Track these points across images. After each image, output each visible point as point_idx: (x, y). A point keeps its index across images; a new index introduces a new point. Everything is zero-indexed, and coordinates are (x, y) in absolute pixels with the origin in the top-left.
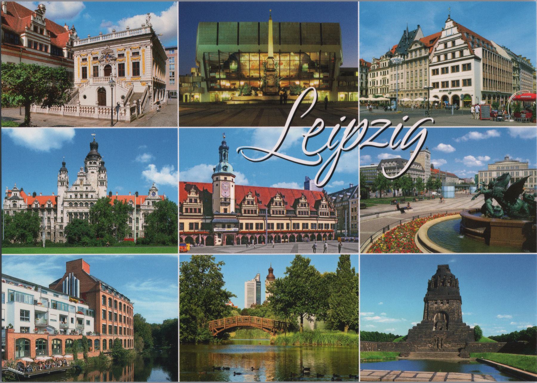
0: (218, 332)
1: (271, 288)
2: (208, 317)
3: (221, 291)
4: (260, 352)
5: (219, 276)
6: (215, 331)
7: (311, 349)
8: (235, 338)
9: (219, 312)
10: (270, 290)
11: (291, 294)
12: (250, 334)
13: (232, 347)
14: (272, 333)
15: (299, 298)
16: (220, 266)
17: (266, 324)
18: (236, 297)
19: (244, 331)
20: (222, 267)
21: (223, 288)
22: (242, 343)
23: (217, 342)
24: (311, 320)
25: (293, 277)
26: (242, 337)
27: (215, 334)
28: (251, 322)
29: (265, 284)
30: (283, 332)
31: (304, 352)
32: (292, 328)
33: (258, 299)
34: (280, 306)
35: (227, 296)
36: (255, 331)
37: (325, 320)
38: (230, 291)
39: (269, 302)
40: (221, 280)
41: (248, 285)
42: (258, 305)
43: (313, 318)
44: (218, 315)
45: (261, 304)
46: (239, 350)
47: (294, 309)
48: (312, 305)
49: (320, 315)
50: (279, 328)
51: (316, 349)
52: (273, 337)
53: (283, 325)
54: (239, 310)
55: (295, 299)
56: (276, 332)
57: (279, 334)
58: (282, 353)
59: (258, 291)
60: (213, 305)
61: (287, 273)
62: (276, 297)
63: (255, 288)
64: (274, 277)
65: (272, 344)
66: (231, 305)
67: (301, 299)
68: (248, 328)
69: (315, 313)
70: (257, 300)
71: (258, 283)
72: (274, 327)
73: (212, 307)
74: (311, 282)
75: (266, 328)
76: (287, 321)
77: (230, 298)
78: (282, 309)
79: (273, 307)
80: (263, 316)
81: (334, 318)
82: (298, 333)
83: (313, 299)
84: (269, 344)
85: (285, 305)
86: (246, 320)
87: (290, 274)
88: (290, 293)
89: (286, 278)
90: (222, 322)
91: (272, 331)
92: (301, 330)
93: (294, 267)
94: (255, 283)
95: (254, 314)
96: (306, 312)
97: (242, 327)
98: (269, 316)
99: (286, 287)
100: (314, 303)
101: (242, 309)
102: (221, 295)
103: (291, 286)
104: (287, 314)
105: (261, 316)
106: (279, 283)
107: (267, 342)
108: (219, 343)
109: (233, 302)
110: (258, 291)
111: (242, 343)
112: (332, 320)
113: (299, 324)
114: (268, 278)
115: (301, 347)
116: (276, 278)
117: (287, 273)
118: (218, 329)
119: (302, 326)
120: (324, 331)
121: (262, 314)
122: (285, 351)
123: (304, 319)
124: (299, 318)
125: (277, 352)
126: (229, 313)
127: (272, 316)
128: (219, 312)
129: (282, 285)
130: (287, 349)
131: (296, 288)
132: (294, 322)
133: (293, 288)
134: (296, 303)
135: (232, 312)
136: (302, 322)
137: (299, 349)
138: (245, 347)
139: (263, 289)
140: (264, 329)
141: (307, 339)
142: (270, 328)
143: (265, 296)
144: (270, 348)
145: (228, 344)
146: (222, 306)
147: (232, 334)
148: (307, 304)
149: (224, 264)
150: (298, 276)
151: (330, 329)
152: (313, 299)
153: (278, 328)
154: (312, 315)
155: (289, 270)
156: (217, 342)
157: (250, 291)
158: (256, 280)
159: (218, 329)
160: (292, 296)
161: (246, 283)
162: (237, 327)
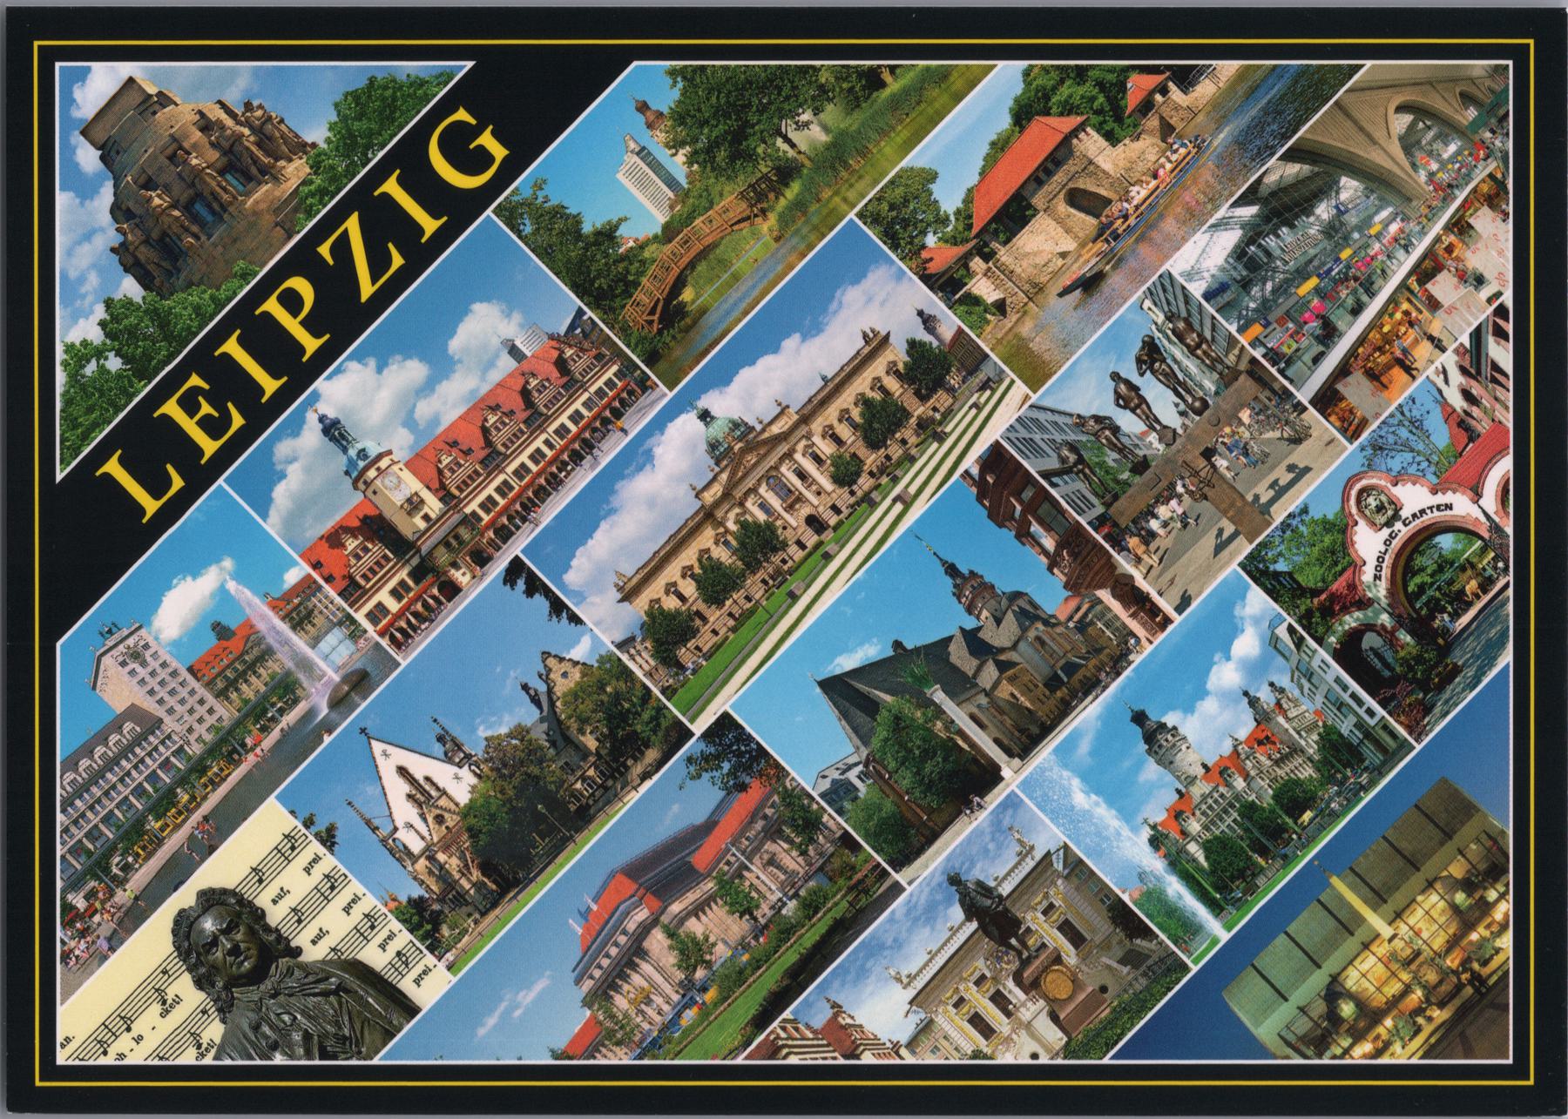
0: (656, 317)
1: (674, 140)
2: (612, 310)
5: (558, 212)
6: (650, 323)
7: (860, 177)
8: (698, 295)
10: (675, 145)
11: (720, 113)
13: (711, 318)
14: (759, 220)
15: (744, 106)
16: (541, 194)
17: (731, 214)
18: (626, 219)
19: (702, 267)
20: (548, 190)
21: (587, 228)
22: (720, 292)
23: (674, 337)
24: (806, 124)
25: (693, 79)
26: (711, 281)
29: (656, 141)
32: (786, 172)
33: (671, 182)
34: (722, 155)
35: (607, 235)
36: (722, 247)
37: (830, 100)
38: (605, 220)
40: (568, 216)
41: (629, 174)
42: (682, 195)
43: (805, 117)
44: (628, 286)
48: (779, 94)
49: (814, 98)
50: (761, 197)
51: (868, 168)
52: (769, 225)
54: (656, 237)
55: (737, 113)
56: (763, 212)
57: (772, 208)
59: (656, 166)
60: (598, 277)
61: (675, 83)
62: (700, 145)
63: (645, 168)
64: (660, 115)
65: (777, 239)
66: (631, 244)
67: (750, 105)
68: (703, 255)
69: (801, 106)
70: (669, 186)
71: (643, 152)
72: (752, 206)
73: (602, 282)
75: (739, 222)
76: (765, 170)
78: (733, 158)
79: (713, 169)
80: (711, 204)
81: (845, 80)
83: (771, 81)
84: (774, 245)
87: (684, 78)
88: (715, 115)
89: (684, 93)
90: (649, 291)
92: (807, 163)
94: (636, 158)
95: (690, 218)
96: (781, 118)
97: (692, 265)
98: (721, 195)
99: (699, 110)
100: (780, 89)
101: (659, 231)
102: (597, 244)
104: (751, 157)
106: (680, 116)
107: (765, 245)
109: (630, 235)
110: (656, 166)
111: (720, 292)
112: (845, 85)
113: (791, 153)
114: (650, 126)
115: (836, 193)
116: (666, 111)
117: (675, 83)
118: (652, 312)
120: (849, 121)
121: (704, 203)
123: (790, 135)
124: (779, 141)
126: (643, 262)
127: (727, 188)
128: (622, 278)
129: (688, 113)
130: (815, 220)
132: (779, 159)
133: (714, 99)
135: (646, 254)
136: (793, 146)
137: (837, 199)
139: (662, 154)
141: (833, 168)
143: (678, 164)
144: (783, 251)
145: (695, 322)
147: (687, 295)
148: (770, 103)
149: (545, 182)
151: (858, 106)
152: (771, 81)
153: (758, 198)
156: (674, 337)
157: (642, 184)
160: (727, 116)
161: (620, 176)
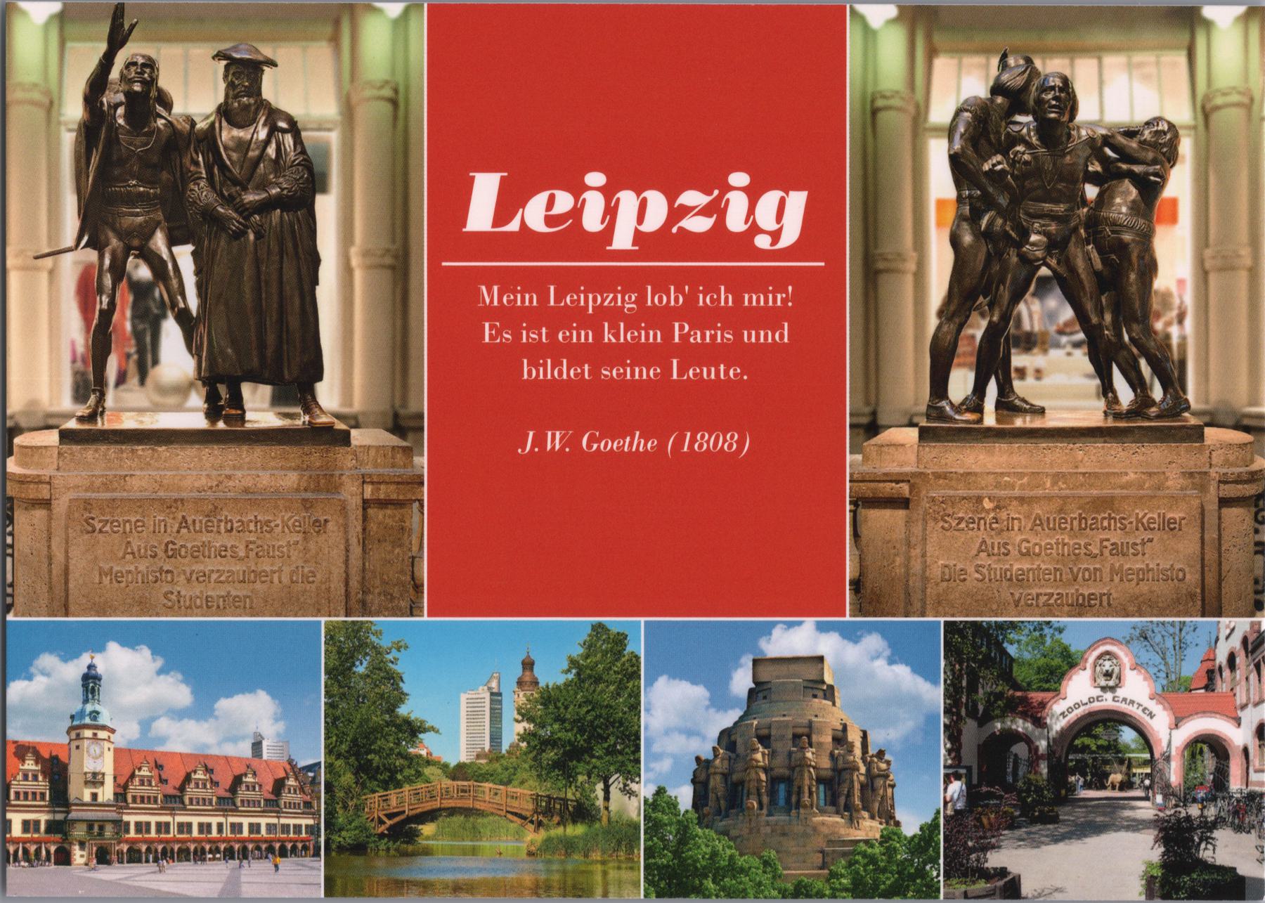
0: (389, 823)
1: (528, 711)
3: (397, 717)
4: (500, 875)
6: (381, 822)
7: (632, 868)
8: (434, 837)
9: (393, 771)
10: (525, 715)
12: (474, 827)
15: (600, 736)
16: (394, 654)
17: (515, 803)
18: (437, 732)
19: (458, 819)
21: (403, 710)
23: (388, 849)
25: (583, 681)
26: (454, 836)
27: (382, 829)
28: (475, 798)
29: (513, 700)
30: (558, 824)
31: (612, 874)
32: (582, 813)
33: (496, 738)
34: (551, 755)
35: (413, 730)
39: (524, 745)
40: (398, 689)
42: (494, 755)
45: (504, 751)
46: (444, 871)
47: (588, 763)
50: (548, 812)
52: (533, 837)
53: (558, 806)
54: (445, 767)
55: (590, 738)
56: (540, 824)
57: (547, 828)
58: (556, 877)
61: (569, 671)
62: (542, 732)
65: (530, 854)
66: (424, 753)
71: (496, 697)
72: (536, 812)
74: (630, 696)
75: (516, 814)
76: (570, 796)
77: (421, 736)
78: (556, 765)
79: (535, 759)
82: (597, 825)
84: (524, 855)
85: (565, 753)
86: (463, 791)
87: (578, 674)
91: (532, 822)
93: (587, 657)
94: (487, 696)
97: (452, 811)
98: (522, 783)
99: (566, 708)
101: (453, 763)
103: (580, 706)
104: (570, 777)
105: (502, 783)
107: (518, 849)
108: (392, 852)
109: (428, 745)
111: (453, 851)
113: (600, 802)
116: (542, 684)
117: (569, 671)
118: (390, 816)
119: (607, 808)
122: (564, 872)
124: (600, 786)
125: (543, 877)
126: (419, 774)
127: (531, 782)
128: (393, 771)
130: (569, 867)
131: (593, 709)
133: (585, 709)
134: (592, 749)
135: (427, 771)
136: (607, 798)
137: (599, 867)
138: (464, 862)
139: (509, 712)
140: (509, 816)
142: (524, 813)
143: (513, 730)
144: (526, 866)
146: (400, 755)
147: (427, 829)
148: (621, 752)
150: (598, 680)
153: (547, 811)
154: (632, 781)
155: (573, 663)
156: (388, 849)
157: (473, 715)
158: (489, 689)
159: (390, 816)
160: (582, 731)
161: (463, 698)
162: (440, 809)
